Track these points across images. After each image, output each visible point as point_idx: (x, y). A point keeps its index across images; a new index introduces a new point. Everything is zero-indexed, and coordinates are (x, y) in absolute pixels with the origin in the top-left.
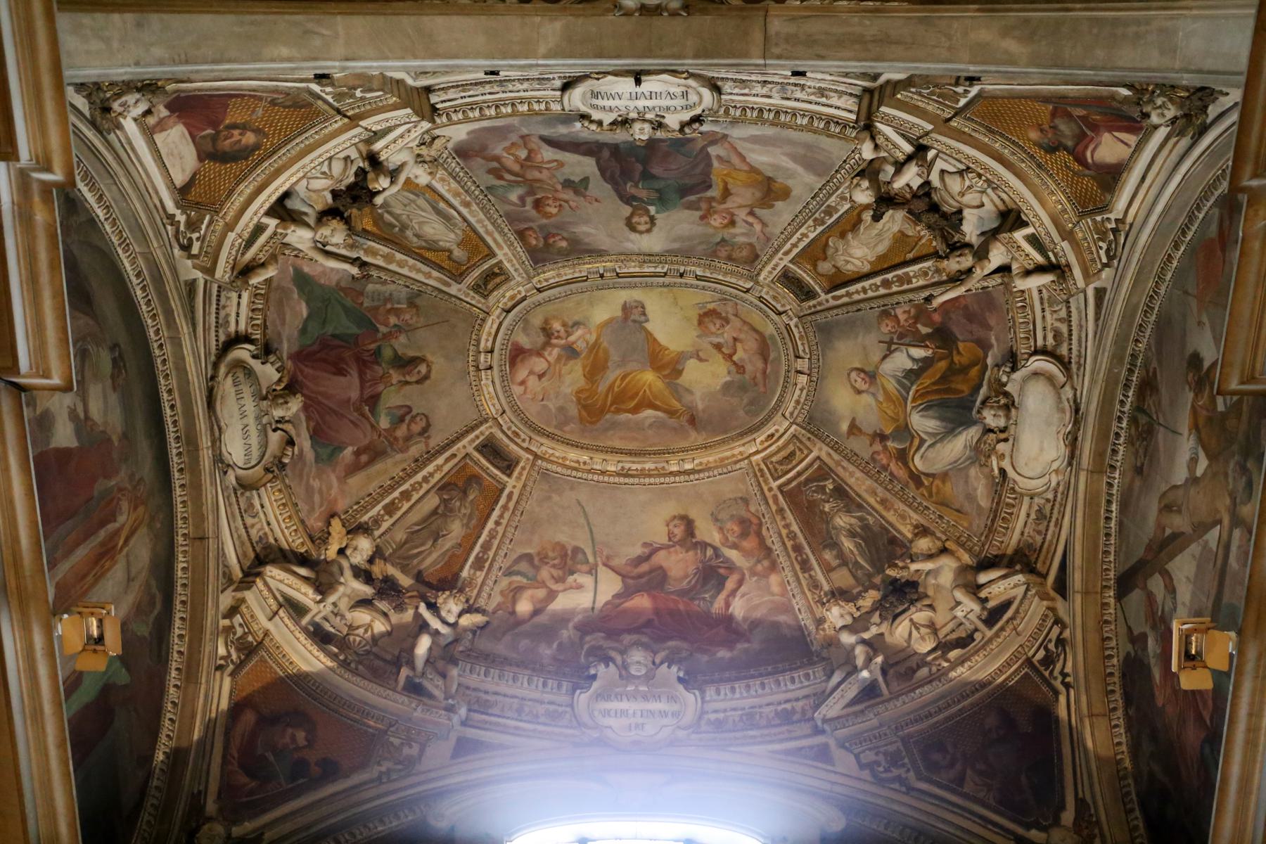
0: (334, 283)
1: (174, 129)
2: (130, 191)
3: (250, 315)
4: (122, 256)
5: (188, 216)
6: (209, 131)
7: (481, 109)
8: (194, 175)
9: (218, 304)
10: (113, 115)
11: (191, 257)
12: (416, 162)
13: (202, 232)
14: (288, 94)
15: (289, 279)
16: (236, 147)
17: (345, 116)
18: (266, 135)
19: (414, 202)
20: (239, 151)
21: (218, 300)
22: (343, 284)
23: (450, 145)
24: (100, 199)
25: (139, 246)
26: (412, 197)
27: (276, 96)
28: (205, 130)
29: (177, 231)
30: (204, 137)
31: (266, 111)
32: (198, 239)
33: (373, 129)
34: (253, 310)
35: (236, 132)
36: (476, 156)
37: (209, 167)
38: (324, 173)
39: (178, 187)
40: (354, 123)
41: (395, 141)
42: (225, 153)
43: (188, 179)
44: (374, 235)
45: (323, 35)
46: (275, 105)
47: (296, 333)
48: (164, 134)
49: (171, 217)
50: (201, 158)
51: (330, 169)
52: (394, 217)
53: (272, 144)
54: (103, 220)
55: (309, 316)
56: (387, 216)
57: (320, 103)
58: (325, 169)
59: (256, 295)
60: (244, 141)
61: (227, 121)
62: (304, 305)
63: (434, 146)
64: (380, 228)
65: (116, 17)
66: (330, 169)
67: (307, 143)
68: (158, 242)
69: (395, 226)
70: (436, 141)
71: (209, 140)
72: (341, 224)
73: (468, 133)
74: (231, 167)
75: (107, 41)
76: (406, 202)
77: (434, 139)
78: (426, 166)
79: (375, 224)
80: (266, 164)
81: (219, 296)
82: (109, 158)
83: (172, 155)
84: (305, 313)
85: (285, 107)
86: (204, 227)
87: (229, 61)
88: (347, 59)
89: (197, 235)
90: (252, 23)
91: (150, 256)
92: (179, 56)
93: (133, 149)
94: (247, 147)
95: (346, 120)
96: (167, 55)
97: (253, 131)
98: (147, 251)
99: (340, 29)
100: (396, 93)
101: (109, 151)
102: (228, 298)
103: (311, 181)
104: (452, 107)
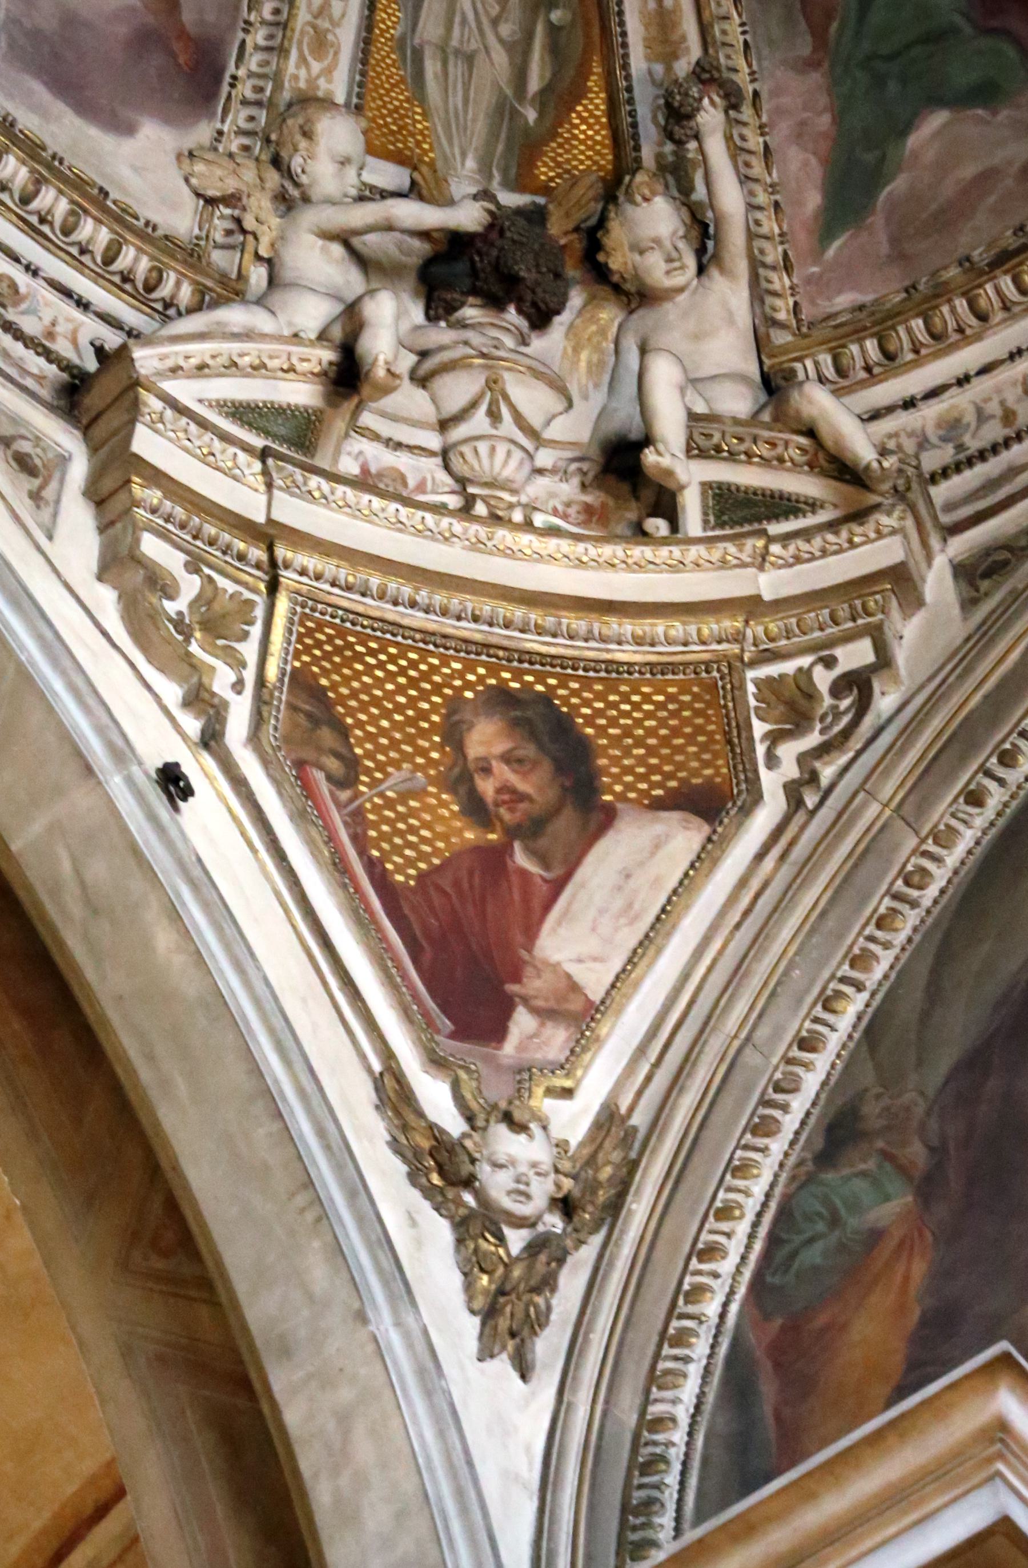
0: (816, 78)
1: (555, 957)
2: (755, 982)
3: (1000, 316)
4: (940, 876)
5: (775, 738)
6: (521, 858)
7: (25, 200)
8: (659, 805)
9: (1007, 443)
10: (567, 1183)
11: (884, 661)
12: (306, 199)
13: (805, 661)
14: (300, 765)
15: (864, 237)
16: (529, 750)
17: (273, 562)
18: (455, 704)
19: (443, 50)
20: (533, 735)
21: (995, 449)
22: (805, 47)
23: (202, 133)
24: (808, 1043)
25: (896, 848)
26: (431, 67)
27: (324, 787)
28: (523, 873)
29: (823, 750)
30: (544, 861)
31: (381, 767)
32: (829, 662)
33: (258, 466)
34: (983, 317)
35: (487, 787)
36: (182, 34)
37: (617, 779)
38: (494, 416)
39: (706, 829)
40: (272, 531)
41: (259, 368)
42: (560, 768)
43: (675, 816)
44: (609, 76)
45: (74, 860)
46: (352, 764)
47: (1004, 115)
48: (580, 974)
49: (793, 792)
50: (608, 818)
51: (474, 405)
52: (527, 53)
53: (470, 666)
54: (865, 996)
55: (936, 100)
56: (534, 84)
57: (272, 673)
58: (479, 422)
59: (935, 337)
60: (501, 747)
61: (469, 835)
62: (913, 141)
63: (231, 185)
64: (583, 73)
65: (293, 1417)
66: (474, 405)
67: (407, 591)
68: (864, 805)
69: (553, 30)
70: (211, 193)
71: (543, 843)
72: (608, 242)
73: (127, 129)
74: (589, 721)
75: (344, 1419)
76: (457, 69)
77: (211, 202)
78: (296, 163)
79: (577, 93)
80: (533, 643)
81: (982, 456)
82: (687, 1101)
83: (630, 905)
84: (938, 119)
85: (344, 732)
86: (789, 667)
87: (256, 1071)
88: (89, 770)
89: (819, 672)
90: (150, 1058)
91: (908, 809)
92: (302, 1211)
93: (685, 977)
94: (515, 724)
95: (282, 552)
96: (316, 1244)
97: (459, 747)
98: (900, 823)
99: (37, 827)
100: (122, 496)
101: (670, 1117)
102: (982, 417)
103: (535, 420)
104: (80, 267)
